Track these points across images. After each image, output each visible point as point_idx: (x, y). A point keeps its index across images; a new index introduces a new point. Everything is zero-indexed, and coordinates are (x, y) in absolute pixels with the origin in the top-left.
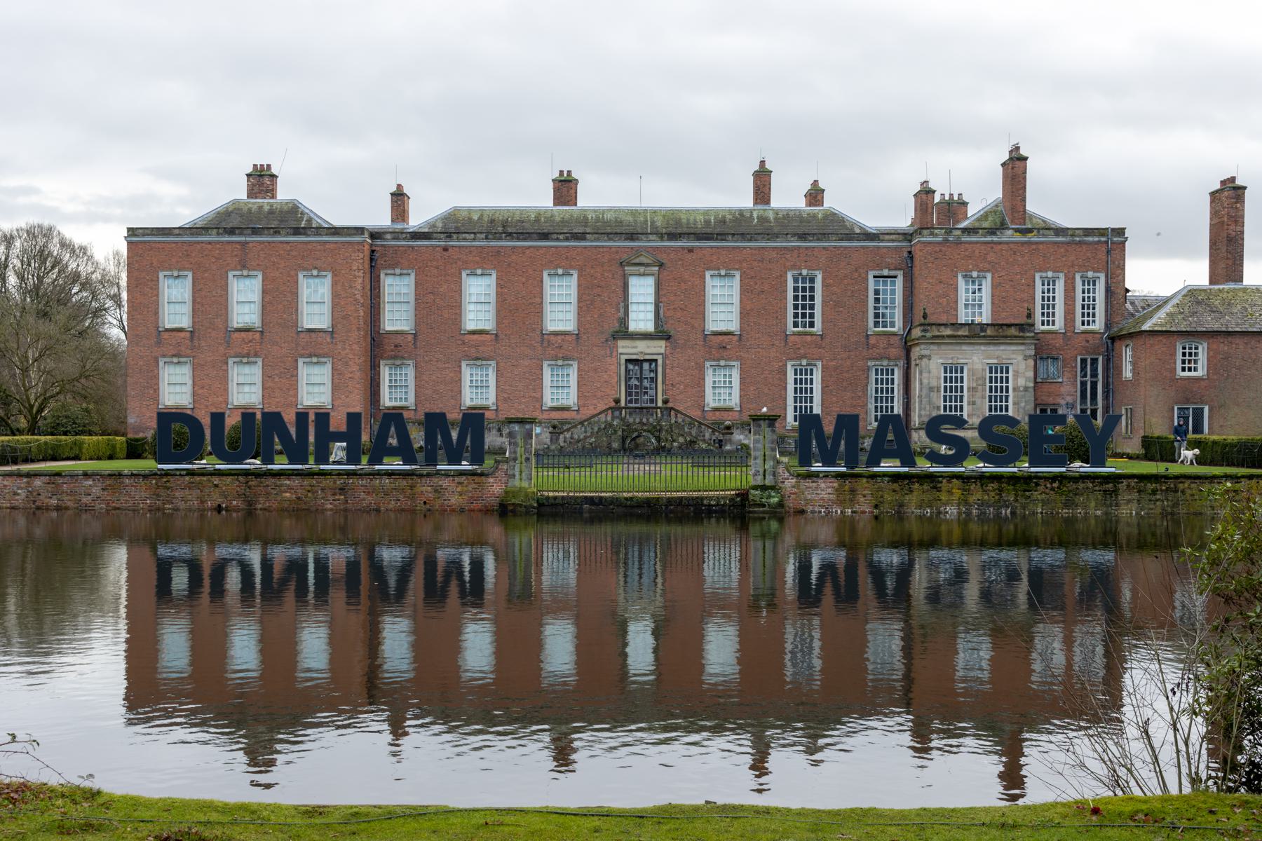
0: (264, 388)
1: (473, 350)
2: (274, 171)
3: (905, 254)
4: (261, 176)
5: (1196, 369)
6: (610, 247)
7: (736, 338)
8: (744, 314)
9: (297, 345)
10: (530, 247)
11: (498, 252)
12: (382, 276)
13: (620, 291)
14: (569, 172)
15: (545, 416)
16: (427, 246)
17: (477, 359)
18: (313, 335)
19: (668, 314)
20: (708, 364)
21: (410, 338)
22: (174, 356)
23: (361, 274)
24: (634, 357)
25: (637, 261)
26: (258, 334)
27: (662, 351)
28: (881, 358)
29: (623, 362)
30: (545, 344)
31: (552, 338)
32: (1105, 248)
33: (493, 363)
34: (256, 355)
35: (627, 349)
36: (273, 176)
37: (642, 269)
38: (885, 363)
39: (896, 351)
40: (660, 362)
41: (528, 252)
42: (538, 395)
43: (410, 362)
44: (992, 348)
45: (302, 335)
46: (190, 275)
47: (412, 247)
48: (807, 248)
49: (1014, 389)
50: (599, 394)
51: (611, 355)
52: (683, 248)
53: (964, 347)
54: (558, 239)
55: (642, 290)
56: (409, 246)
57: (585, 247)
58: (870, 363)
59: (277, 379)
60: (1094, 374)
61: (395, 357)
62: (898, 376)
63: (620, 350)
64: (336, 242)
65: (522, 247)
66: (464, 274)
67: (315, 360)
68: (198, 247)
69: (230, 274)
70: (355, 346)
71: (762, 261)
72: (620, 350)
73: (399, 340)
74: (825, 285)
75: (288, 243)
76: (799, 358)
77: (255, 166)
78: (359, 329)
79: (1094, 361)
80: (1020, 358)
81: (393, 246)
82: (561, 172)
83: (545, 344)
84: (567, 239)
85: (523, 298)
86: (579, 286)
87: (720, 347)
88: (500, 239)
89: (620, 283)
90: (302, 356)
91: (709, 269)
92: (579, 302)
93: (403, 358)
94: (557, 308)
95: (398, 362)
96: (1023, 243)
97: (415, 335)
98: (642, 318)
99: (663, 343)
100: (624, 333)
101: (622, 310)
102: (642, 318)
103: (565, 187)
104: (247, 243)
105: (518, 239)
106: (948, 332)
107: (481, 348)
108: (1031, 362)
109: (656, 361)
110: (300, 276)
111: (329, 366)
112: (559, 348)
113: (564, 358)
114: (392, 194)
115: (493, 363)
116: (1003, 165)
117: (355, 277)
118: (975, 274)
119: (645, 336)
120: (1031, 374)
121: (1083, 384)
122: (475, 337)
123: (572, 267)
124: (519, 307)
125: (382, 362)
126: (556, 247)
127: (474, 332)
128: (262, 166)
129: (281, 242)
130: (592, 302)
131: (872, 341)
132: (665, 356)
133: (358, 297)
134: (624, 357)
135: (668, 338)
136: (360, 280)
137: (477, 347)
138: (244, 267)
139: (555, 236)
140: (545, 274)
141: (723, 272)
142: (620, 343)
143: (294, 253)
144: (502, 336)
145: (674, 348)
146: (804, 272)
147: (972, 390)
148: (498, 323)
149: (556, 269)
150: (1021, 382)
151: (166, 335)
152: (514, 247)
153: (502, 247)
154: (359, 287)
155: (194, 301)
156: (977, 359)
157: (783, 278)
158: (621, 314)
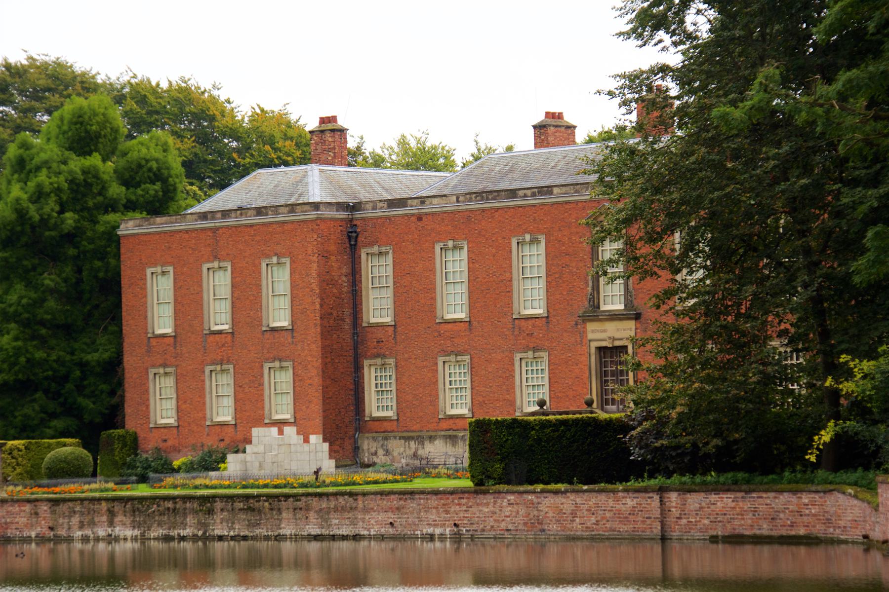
0: (236, 400)
1: (449, 343)
6: (577, 202)
12: (363, 256)
16: (403, 216)
18: (276, 335)
21: (391, 329)
22: (160, 365)
23: (315, 258)
24: (604, 344)
26: (230, 336)
27: (633, 334)
29: (593, 351)
30: (516, 333)
31: (523, 323)
33: (467, 358)
34: (228, 362)
35: (602, 334)
36: (342, 131)
40: (630, 350)
41: (497, 214)
43: (391, 361)
45: (267, 335)
46: (170, 269)
47: (388, 218)
57: (552, 204)
59: (246, 390)
61: (377, 356)
63: (590, 336)
64: (293, 222)
65: (491, 209)
70: (313, 346)
72: (590, 336)
73: (380, 334)
75: (251, 226)
78: (315, 325)
81: (372, 219)
83: (516, 333)
84: (534, 195)
86: (547, 255)
88: (470, 200)
90: (267, 360)
92: (548, 275)
93: (384, 356)
94: (528, 284)
95: (379, 361)
99: (631, 324)
100: (594, 313)
101: (590, 284)
104: (217, 229)
109: (626, 347)
111: (291, 371)
112: (530, 335)
113: (535, 350)
114: (535, 127)
115: (467, 358)
117: (311, 262)
119: (614, 316)
122: (450, 326)
123: (540, 232)
124: (491, 287)
125: (366, 363)
127: (448, 322)
129: (246, 226)
132: (634, 341)
133: (314, 286)
134: (594, 345)
135: (637, 317)
136: (315, 266)
137: (451, 339)
139: (521, 193)
142: (591, 326)
143: (257, 238)
144: (475, 323)
149: (523, 235)
151: (154, 342)
152: (483, 210)
153: (471, 211)
154: (314, 274)
155: (176, 301)
158: (590, 289)
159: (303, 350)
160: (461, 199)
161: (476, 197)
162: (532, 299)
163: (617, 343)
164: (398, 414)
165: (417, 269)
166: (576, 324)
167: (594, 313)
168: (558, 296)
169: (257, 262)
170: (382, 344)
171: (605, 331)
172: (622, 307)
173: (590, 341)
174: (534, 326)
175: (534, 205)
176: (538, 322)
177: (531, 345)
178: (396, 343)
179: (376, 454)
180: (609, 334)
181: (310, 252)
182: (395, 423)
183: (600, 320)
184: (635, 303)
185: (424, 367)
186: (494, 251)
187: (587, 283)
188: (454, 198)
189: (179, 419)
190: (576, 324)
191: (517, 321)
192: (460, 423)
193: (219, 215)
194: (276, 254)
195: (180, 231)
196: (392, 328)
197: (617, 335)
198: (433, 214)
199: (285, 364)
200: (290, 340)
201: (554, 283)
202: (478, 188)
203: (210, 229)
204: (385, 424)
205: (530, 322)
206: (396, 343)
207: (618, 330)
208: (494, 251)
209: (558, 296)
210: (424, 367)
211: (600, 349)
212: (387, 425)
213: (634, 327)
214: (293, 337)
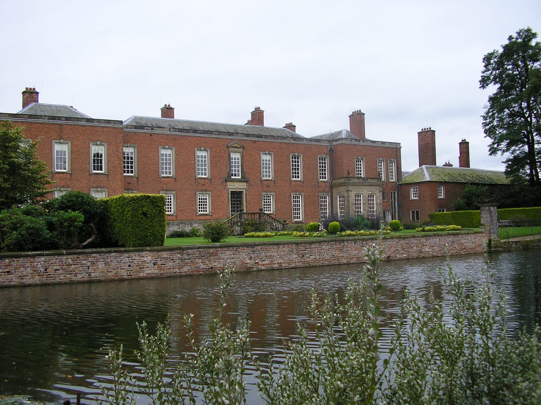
2: (37, 90)
4: (32, 93)
5: (171, 211)
8: (276, 171)
9: (90, 181)
11: (175, 138)
14: (169, 105)
17: (166, 190)
18: (98, 176)
19: (247, 170)
21: (135, 179)
25: (234, 146)
28: (323, 192)
29: (230, 192)
31: (200, 180)
37: (236, 149)
39: (327, 189)
40: (244, 192)
41: (188, 138)
44: (370, 187)
45: (92, 176)
48: (297, 144)
50: (221, 207)
52: (251, 141)
53: (362, 187)
54: (201, 133)
57: (213, 138)
60: (395, 199)
63: (229, 187)
66: (160, 147)
67: (99, 189)
68: (36, 125)
69: (53, 142)
71: (280, 148)
72: (229, 187)
74: (303, 160)
76: (296, 191)
77: (27, 88)
79: (394, 193)
82: (166, 105)
87: (267, 186)
88: (176, 131)
89: (228, 156)
90: (92, 187)
93: (132, 190)
96: (373, 147)
98: (237, 172)
99: (245, 184)
102: (237, 172)
103: (168, 111)
104: (63, 125)
106: (357, 180)
107: (168, 185)
108: (381, 193)
109: (242, 192)
110: (91, 144)
112: (203, 186)
118: (360, 158)
120: (381, 198)
121: (392, 202)
122: (166, 179)
124: (185, 165)
126: (200, 137)
128: (30, 89)
130: (216, 163)
131: (320, 184)
134: (230, 190)
135: (247, 182)
138: (61, 138)
140: (196, 149)
141: (267, 152)
142: (229, 183)
145: (250, 186)
146: (296, 154)
150: (379, 201)
152: (182, 136)
153: (176, 135)
156: (365, 192)
157: (289, 155)
159: (114, 184)
160: (171, 130)
167: (228, 179)
169: (87, 142)
172: (240, 177)
175: (205, 137)
180: (236, 187)
181: (118, 141)
193: (64, 119)
194: (99, 141)
195: (38, 123)
198: (158, 134)
199: (103, 189)
200: (106, 179)
202: (180, 127)
203: (58, 124)
214: (108, 178)
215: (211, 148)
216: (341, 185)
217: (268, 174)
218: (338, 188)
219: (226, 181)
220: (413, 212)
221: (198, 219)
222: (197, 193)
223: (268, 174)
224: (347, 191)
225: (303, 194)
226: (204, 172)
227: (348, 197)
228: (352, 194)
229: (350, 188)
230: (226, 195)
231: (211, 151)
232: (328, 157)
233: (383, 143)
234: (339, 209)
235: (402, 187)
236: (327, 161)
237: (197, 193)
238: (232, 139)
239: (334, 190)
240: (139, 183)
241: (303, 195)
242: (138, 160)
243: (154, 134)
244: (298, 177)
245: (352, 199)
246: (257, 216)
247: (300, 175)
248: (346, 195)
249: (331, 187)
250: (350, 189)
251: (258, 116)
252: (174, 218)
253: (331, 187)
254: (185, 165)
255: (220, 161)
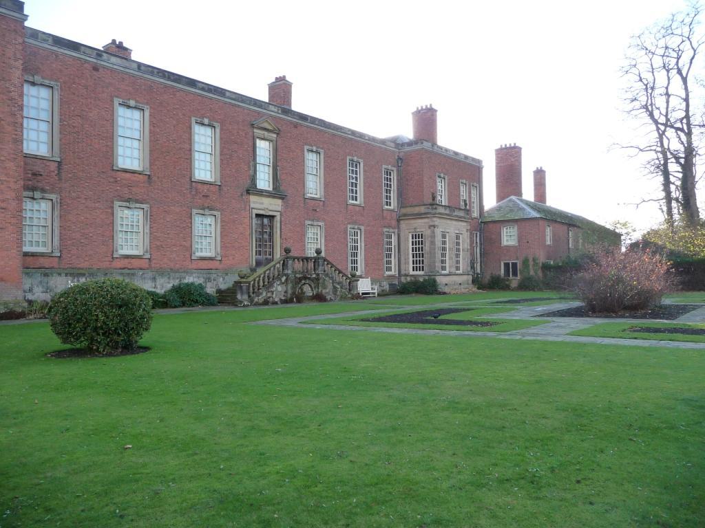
1: (126, 190)
3: (396, 157)
7: (321, 203)
10: (181, 90)
13: (250, 149)
15: (194, 266)
17: (128, 200)
20: (308, 222)
21: (53, 166)
23: (19, 64)
25: (262, 125)
27: (279, 209)
28: (389, 227)
29: (254, 216)
30: (193, 193)
32: (469, 170)
38: (391, 230)
39: (394, 223)
40: (278, 218)
42: (187, 244)
43: (53, 196)
49: (463, 250)
51: (245, 208)
52: (291, 122)
53: (449, 222)
55: (264, 149)
56: (53, 52)
58: (385, 230)
62: (394, 240)
63: (252, 205)
66: (116, 101)
72: (252, 205)
73: (38, 168)
74: (365, 171)
76: (355, 223)
80: (465, 230)
85: (174, 141)
87: (313, 209)
89: (251, 144)
91: (306, 144)
93: (43, 191)
97: (59, 163)
99: (279, 202)
100: (252, 190)
101: (252, 168)
105: (169, 79)
107: (134, 189)
109: (273, 217)
112: (204, 197)
116: (413, 113)
122: (128, 175)
127: (126, 171)
134: (255, 212)
135: (282, 197)
137: (129, 188)
142: (253, 198)
144: (155, 178)
146: (355, 159)
147: (450, 249)
148: (151, 164)
152: (166, 86)
153: (154, 82)
157: (344, 159)
158: (251, 172)
161: (158, 73)
162: (204, 168)
163: (271, 213)
164: (60, 251)
165: (91, 115)
166: (242, 195)
168: (229, 172)
170: (40, 178)
171: (262, 204)
172: (271, 189)
173: (252, 208)
174: (208, 190)
175: (211, 99)
176: (212, 188)
177: (206, 205)
178: (60, 179)
179: (31, 290)
182: (57, 259)
183: (262, 195)
184: (282, 188)
185: (95, 208)
186: (174, 122)
187: (250, 169)
188: (135, 66)
189: (519, 241)
190: (242, 195)
191: (194, 184)
192: (136, 263)
196: (56, 164)
197: (271, 208)
198: (112, 71)
201: (225, 162)
204: (42, 261)
205: (206, 187)
206: (60, 179)
207: (271, 204)
208: (174, 122)
209: (229, 172)
210: (95, 208)
211: (258, 216)
212: (42, 261)
213: (281, 204)
215: (222, 123)
216: (419, 216)
217: (314, 186)
218: (413, 221)
219: (248, 192)
220: (507, 265)
221: (194, 266)
222: (195, 211)
223: (314, 186)
224: (430, 227)
225: (362, 228)
226: (204, 168)
227: (433, 236)
228: (438, 232)
229: (437, 221)
230: (247, 220)
231: (221, 130)
232: (395, 169)
233: (466, 157)
234: (411, 256)
235: (486, 228)
236: (394, 176)
237: (195, 211)
238: (259, 113)
239: (403, 224)
240: (64, 175)
241: (363, 230)
242: (61, 120)
243: (104, 67)
244: (356, 200)
245: (439, 239)
246: (311, 265)
247: (358, 195)
248: (427, 232)
249: (398, 221)
250: (436, 223)
251: (281, 89)
252: (144, 264)
253: (398, 221)
254: (169, 150)
255: (235, 154)
